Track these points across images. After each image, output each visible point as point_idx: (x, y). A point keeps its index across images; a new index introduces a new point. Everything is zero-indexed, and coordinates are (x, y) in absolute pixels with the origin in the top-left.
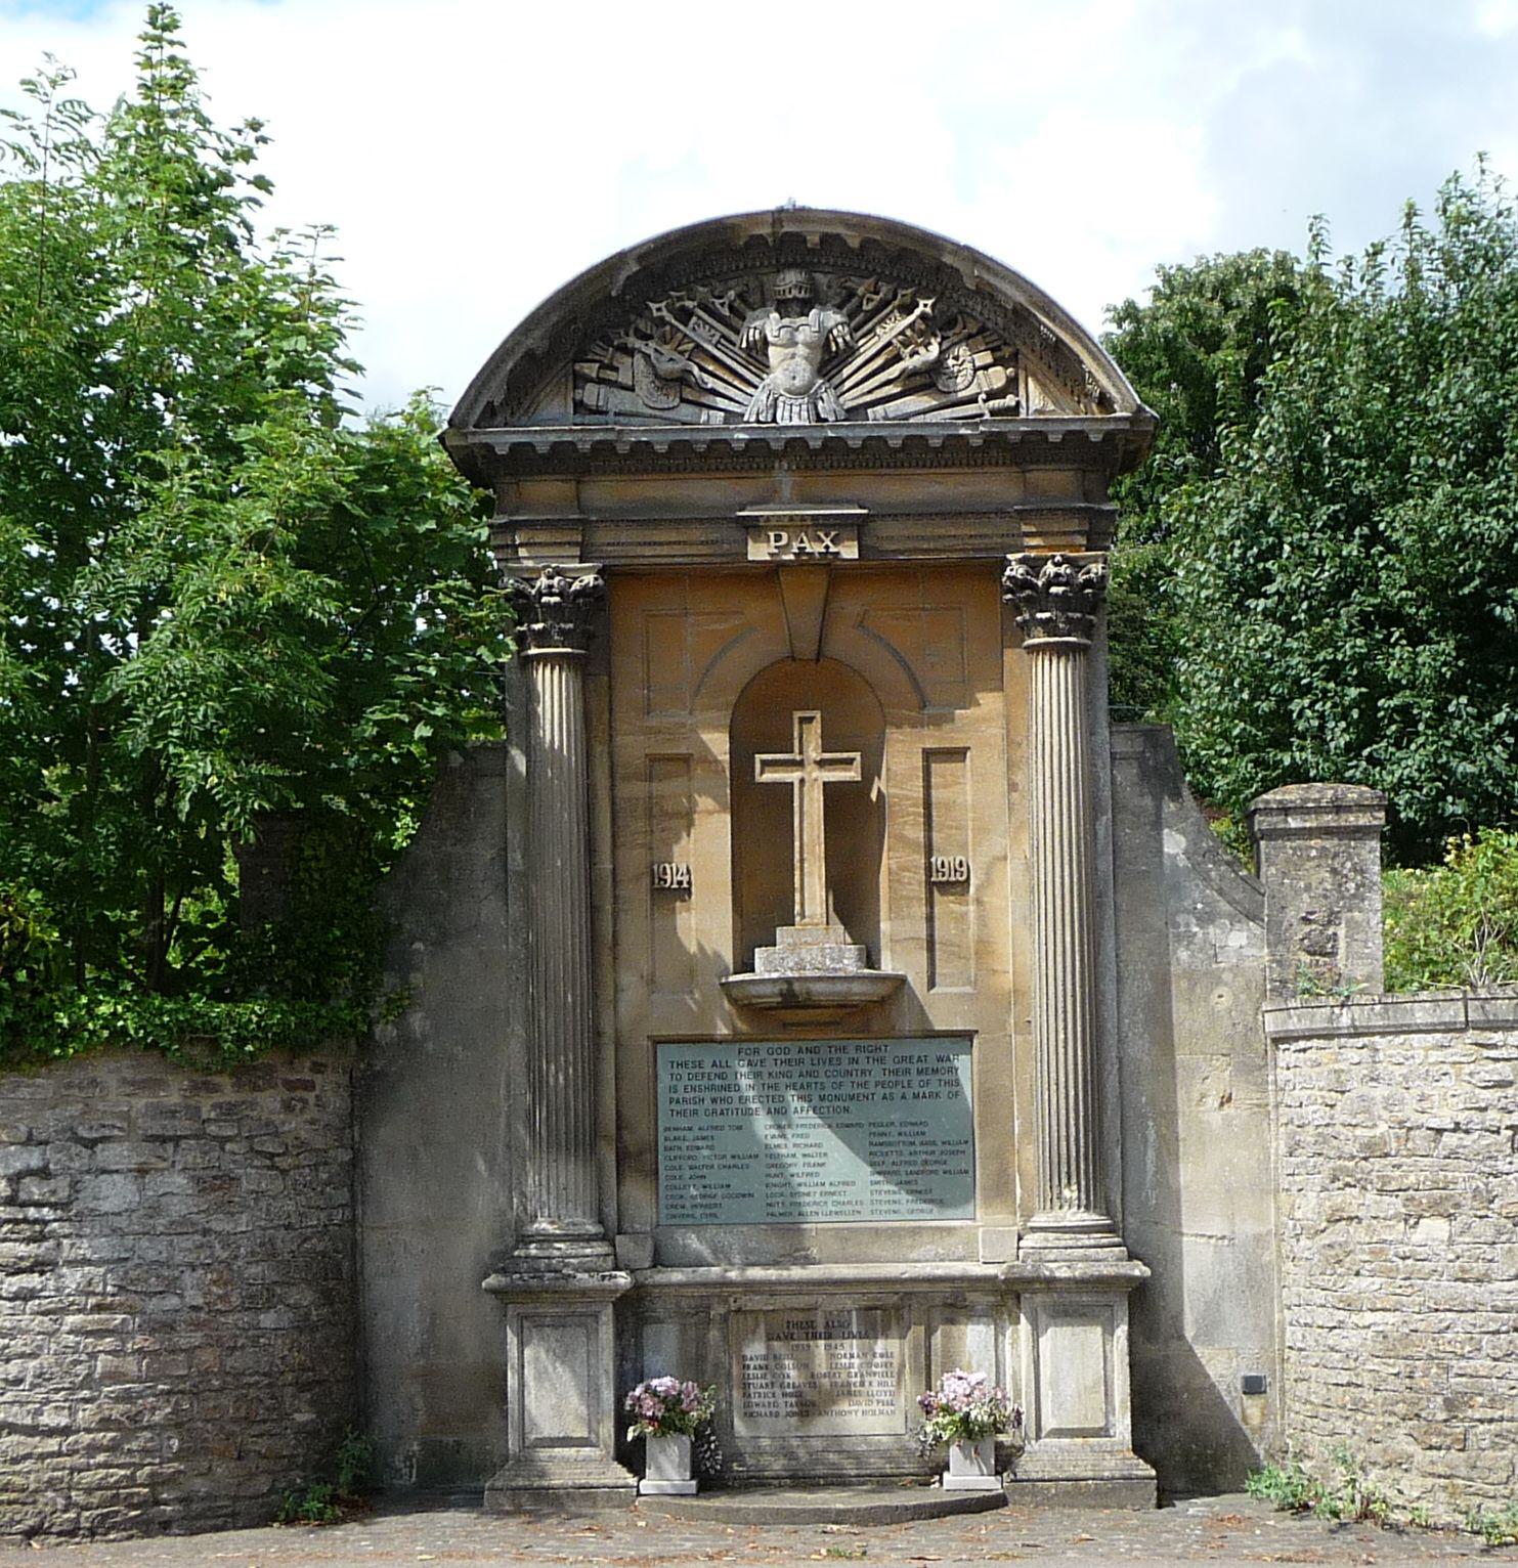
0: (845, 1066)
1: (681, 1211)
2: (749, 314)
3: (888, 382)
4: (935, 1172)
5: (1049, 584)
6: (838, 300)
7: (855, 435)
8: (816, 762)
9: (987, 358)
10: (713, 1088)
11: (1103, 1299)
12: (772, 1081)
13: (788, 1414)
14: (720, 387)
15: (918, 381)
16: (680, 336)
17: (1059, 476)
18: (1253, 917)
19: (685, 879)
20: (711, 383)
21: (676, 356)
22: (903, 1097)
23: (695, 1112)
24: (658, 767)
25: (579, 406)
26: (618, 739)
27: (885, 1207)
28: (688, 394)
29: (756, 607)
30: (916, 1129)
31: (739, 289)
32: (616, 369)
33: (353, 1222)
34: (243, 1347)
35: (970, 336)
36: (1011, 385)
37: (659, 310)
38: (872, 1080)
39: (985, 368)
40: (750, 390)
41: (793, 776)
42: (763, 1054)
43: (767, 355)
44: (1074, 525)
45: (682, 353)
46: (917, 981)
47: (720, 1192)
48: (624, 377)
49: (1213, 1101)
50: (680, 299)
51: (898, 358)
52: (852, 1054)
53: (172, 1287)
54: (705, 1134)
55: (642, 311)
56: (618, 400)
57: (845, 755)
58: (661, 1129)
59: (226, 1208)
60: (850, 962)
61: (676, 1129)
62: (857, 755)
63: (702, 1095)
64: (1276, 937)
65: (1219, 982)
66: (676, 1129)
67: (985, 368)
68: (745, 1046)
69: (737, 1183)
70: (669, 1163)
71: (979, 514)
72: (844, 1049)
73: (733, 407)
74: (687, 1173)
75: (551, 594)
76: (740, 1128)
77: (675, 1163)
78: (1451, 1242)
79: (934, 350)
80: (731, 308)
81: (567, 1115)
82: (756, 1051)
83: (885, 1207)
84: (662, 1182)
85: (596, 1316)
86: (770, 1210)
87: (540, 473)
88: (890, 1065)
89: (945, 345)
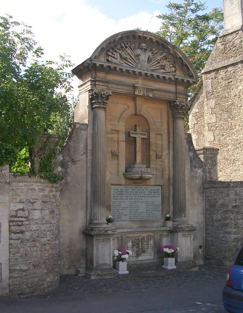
5: (182, 106)
9: (171, 66)
11: (189, 233)
14: (131, 62)
15: (162, 67)
17: (182, 88)
20: (129, 60)
25: (108, 60)
44: (184, 97)
48: (116, 56)
49: (196, 199)
51: (159, 63)
56: (114, 60)
65: (197, 178)
75: (104, 95)
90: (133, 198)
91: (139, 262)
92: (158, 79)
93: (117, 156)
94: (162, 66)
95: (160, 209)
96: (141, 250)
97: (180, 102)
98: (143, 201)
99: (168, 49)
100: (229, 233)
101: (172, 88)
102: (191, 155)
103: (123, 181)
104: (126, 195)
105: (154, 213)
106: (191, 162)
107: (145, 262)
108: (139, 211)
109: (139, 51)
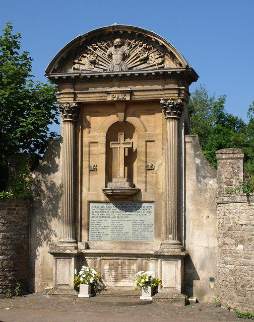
3: (137, 62)
5: (169, 104)
12: (113, 211)
14: (103, 64)
18: (214, 177)
20: (101, 63)
24: (91, 144)
25: (74, 69)
28: (96, 66)
33: (28, 238)
35: (154, 52)
36: (163, 62)
39: (157, 58)
41: (118, 146)
46: (143, 191)
49: (205, 217)
51: (139, 57)
56: (82, 67)
60: (126, 185)
64: (219, 182)
67: (157, 58)
69: (105, 232)
72: (128, 204)
73: (106, 68)
75: (66, 108)
78: (244, 250)
79: (146, 55)
80: (105, 47)
90: (116, 216)
91: (116, 289)
93: (96, 170)
95: (152, 229)
96: (120, 275)
98: (128, 219)
103: (103, 198)
105: (143, 233)
106: (198, 171)
107: (125, 289)
108: (123, 231)
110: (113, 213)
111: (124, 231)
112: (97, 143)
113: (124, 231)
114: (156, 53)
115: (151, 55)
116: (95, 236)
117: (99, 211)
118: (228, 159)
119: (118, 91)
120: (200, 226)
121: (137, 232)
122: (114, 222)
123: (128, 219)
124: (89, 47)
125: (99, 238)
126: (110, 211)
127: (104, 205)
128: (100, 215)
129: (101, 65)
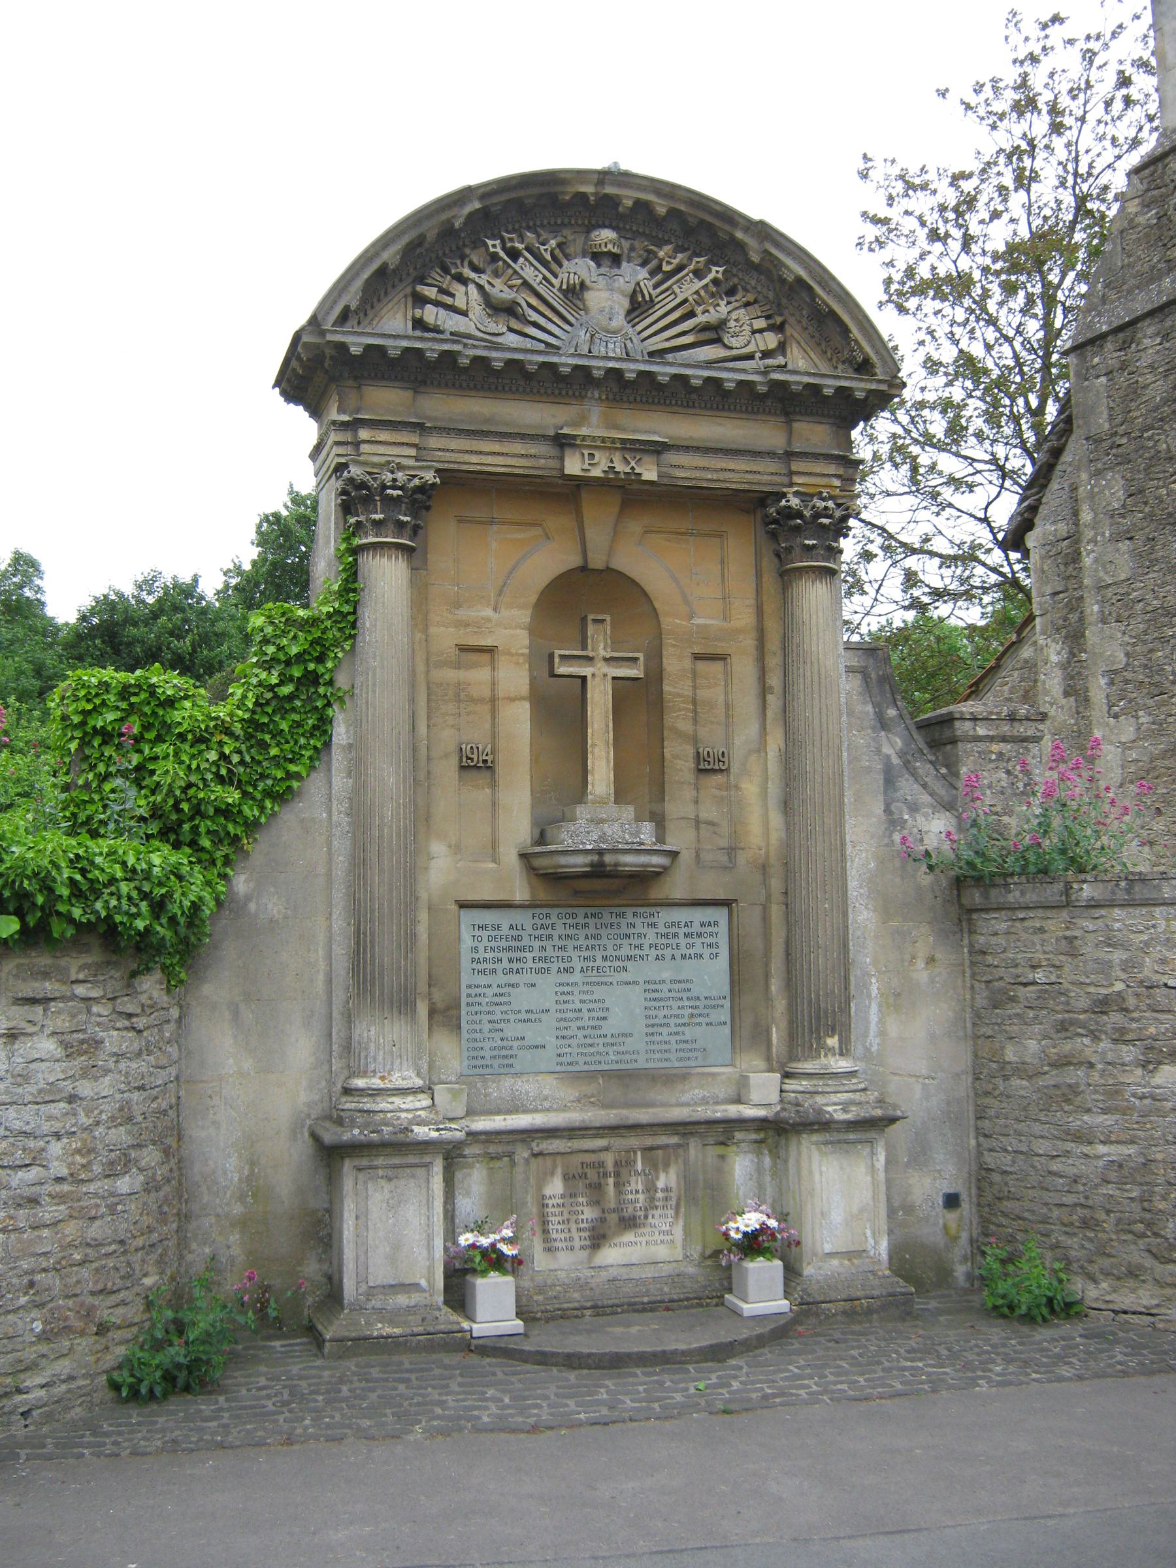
0: (624, 930)
1: (479, 1062)
2: (565, 263)
4: (700, 1024)
6: (640, 261)
7: (664, 371)
8: (606, 660)
9: (761, 323)
10: (510, 949)
12: (561, 943)
13: (582, 1248)
14: (542, 321)
16: (510, 271)
19: (489, 758)
20: (534, 317)
21: (506, 289)
22: (673, 957)
23: (494, 971)
25: (419, 324)
26: (433, 630)
27: (657, 1056)
29: (558, 522)
30: (683, 986)
31: (560, 239)
32: (452, 295)
34: (102, 1216)
35: (747, 305)
36: (782, 348)
37: (494, 246)
38: (646, 943)
39: (760, 331)
40: (567, 327)
42: (554, 919)
43: (582, 300)
44: (832, 469)
45: (510, 287)
47: (516, 1044)
48: (460, 302)
49: (920, 964)
50: (511, 240)
51: (691, 314)
52: (630, 919)
53: (36, 1159)
54: (502, 991)
55: (478, 244)
56: (452, 323)
57: (631, 655)
58: (463, 987)
59: (87, 1073)
61: (477, 986)
62: (640, 656)
63: (500, 955)
66: (477, 986)
67: (760, 331)
68: (538, 911)
69: (531, 1034)
70: (470, 1018)
71: (755, 454)
74: (487, 1027)
75: (394, 488)
76: (534, 985)
77: (476, 1018)
81: (399, 976)
82: (548, 916)
83: (657, 1056)
84: (465, 1035)
85: (427, 1166)
86: (560, 1059)
87: (383, 378)
88: (663, 930)
89: (730, 307)
92: (680, 395)
93: (488, 767)
94: (706, 328)
95: (724, 1015)
97: (805, 497)
99: (741, 246)
100: (1082, 1137)
101: (766, 434)
102: (887, 750)
103: (520, 893)
104: (536, 953)
106: (889, 781)
107: (636, 1273)
109: (580, 268)
110: (561, 953)
111: (617, 1021)
112: (490, 650)
113: (617, 1021)
114: (755, 310)
115: (734, 316)
116: (487, 1054)
117: (504, 944)
118: (991, 739)
119: (613, 440)
120: (898, 999)
121: (665, 1031)
122: (566, 989)
123: (624, 976)
124: (490, 243)
125: (504, 1061)
126: (548, 944)
127: (523, 918)
128: (505, 964)
129: (535, 325)
